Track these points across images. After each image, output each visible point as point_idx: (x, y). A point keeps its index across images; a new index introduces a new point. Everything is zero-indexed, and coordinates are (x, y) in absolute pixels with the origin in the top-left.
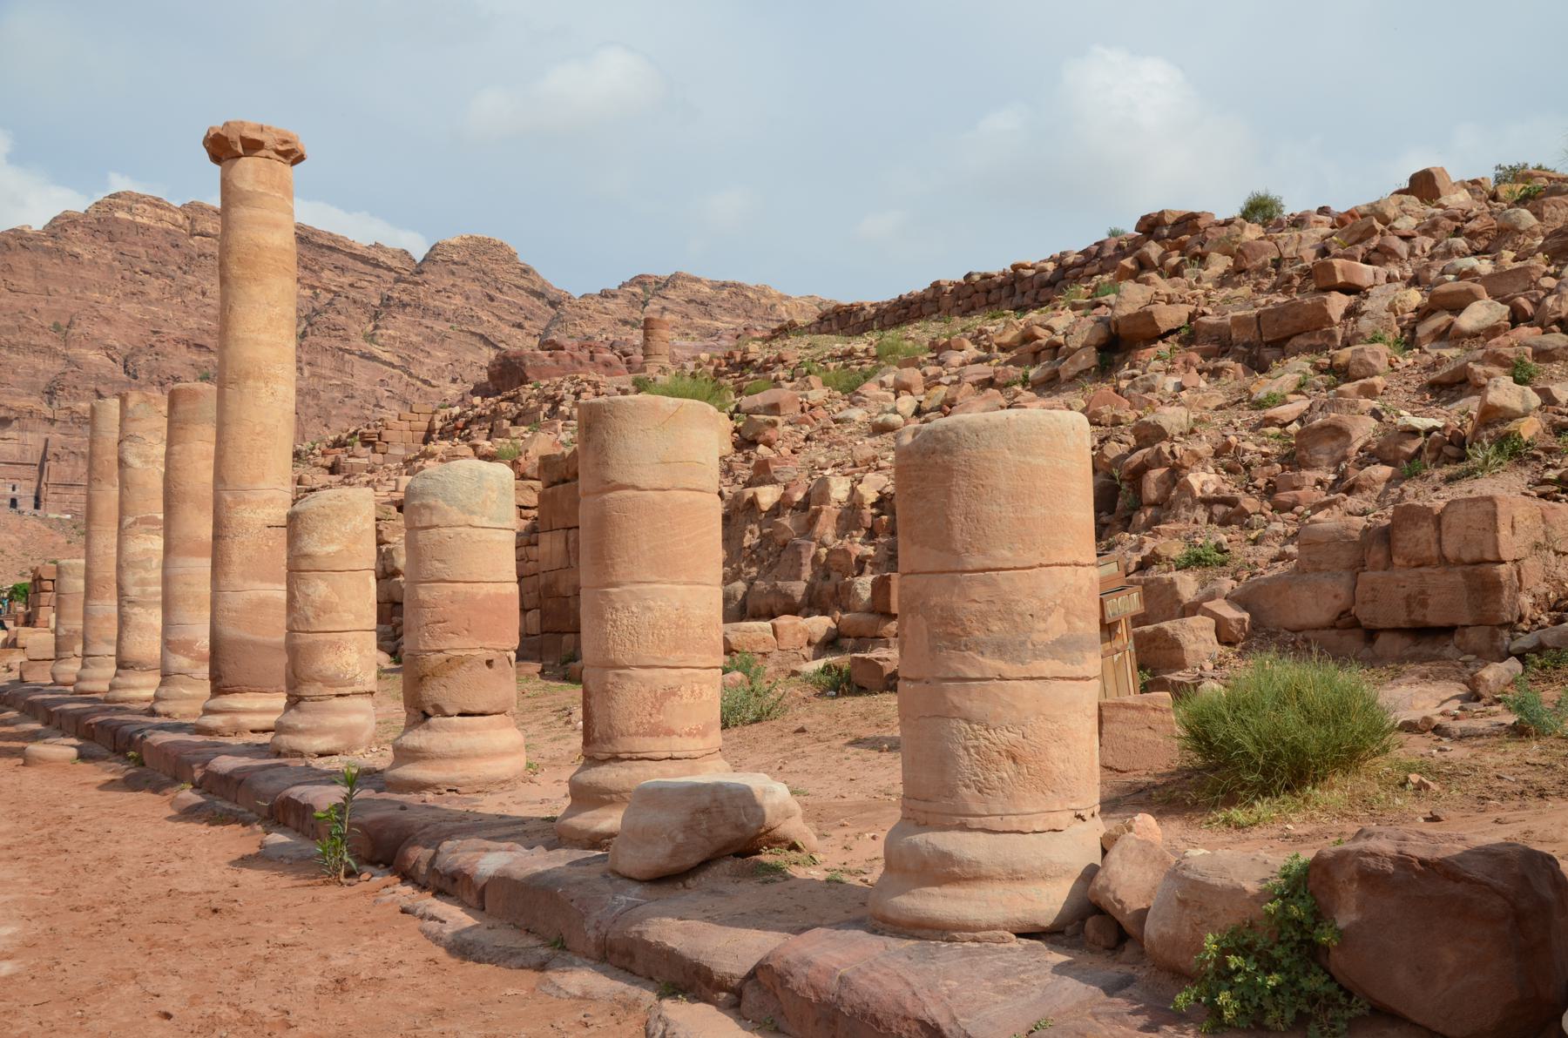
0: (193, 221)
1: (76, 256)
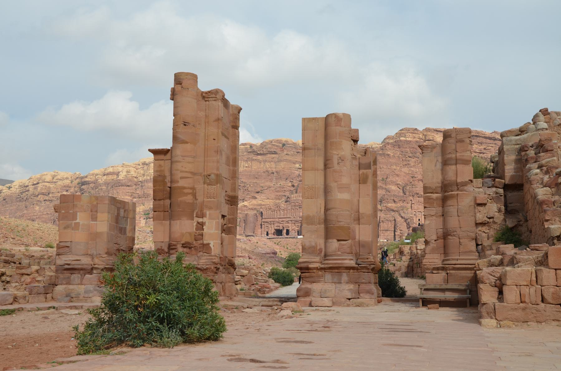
0: (426, 136)
1: (388, 155)
